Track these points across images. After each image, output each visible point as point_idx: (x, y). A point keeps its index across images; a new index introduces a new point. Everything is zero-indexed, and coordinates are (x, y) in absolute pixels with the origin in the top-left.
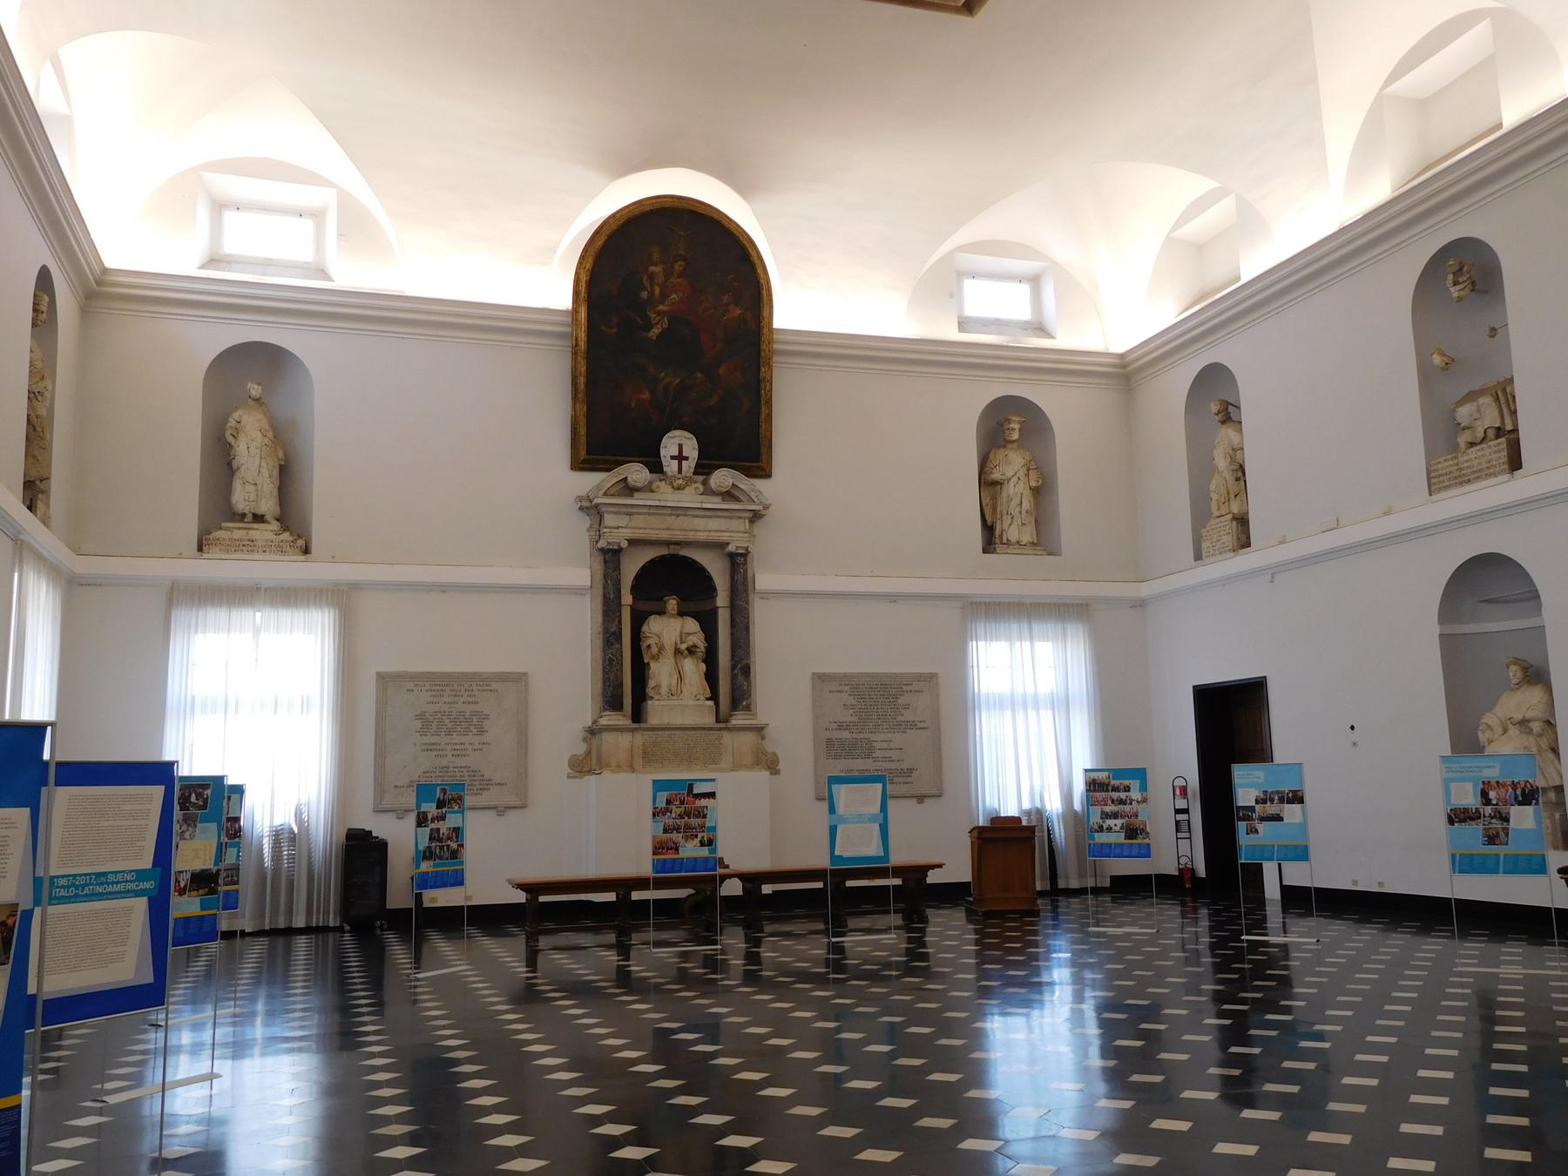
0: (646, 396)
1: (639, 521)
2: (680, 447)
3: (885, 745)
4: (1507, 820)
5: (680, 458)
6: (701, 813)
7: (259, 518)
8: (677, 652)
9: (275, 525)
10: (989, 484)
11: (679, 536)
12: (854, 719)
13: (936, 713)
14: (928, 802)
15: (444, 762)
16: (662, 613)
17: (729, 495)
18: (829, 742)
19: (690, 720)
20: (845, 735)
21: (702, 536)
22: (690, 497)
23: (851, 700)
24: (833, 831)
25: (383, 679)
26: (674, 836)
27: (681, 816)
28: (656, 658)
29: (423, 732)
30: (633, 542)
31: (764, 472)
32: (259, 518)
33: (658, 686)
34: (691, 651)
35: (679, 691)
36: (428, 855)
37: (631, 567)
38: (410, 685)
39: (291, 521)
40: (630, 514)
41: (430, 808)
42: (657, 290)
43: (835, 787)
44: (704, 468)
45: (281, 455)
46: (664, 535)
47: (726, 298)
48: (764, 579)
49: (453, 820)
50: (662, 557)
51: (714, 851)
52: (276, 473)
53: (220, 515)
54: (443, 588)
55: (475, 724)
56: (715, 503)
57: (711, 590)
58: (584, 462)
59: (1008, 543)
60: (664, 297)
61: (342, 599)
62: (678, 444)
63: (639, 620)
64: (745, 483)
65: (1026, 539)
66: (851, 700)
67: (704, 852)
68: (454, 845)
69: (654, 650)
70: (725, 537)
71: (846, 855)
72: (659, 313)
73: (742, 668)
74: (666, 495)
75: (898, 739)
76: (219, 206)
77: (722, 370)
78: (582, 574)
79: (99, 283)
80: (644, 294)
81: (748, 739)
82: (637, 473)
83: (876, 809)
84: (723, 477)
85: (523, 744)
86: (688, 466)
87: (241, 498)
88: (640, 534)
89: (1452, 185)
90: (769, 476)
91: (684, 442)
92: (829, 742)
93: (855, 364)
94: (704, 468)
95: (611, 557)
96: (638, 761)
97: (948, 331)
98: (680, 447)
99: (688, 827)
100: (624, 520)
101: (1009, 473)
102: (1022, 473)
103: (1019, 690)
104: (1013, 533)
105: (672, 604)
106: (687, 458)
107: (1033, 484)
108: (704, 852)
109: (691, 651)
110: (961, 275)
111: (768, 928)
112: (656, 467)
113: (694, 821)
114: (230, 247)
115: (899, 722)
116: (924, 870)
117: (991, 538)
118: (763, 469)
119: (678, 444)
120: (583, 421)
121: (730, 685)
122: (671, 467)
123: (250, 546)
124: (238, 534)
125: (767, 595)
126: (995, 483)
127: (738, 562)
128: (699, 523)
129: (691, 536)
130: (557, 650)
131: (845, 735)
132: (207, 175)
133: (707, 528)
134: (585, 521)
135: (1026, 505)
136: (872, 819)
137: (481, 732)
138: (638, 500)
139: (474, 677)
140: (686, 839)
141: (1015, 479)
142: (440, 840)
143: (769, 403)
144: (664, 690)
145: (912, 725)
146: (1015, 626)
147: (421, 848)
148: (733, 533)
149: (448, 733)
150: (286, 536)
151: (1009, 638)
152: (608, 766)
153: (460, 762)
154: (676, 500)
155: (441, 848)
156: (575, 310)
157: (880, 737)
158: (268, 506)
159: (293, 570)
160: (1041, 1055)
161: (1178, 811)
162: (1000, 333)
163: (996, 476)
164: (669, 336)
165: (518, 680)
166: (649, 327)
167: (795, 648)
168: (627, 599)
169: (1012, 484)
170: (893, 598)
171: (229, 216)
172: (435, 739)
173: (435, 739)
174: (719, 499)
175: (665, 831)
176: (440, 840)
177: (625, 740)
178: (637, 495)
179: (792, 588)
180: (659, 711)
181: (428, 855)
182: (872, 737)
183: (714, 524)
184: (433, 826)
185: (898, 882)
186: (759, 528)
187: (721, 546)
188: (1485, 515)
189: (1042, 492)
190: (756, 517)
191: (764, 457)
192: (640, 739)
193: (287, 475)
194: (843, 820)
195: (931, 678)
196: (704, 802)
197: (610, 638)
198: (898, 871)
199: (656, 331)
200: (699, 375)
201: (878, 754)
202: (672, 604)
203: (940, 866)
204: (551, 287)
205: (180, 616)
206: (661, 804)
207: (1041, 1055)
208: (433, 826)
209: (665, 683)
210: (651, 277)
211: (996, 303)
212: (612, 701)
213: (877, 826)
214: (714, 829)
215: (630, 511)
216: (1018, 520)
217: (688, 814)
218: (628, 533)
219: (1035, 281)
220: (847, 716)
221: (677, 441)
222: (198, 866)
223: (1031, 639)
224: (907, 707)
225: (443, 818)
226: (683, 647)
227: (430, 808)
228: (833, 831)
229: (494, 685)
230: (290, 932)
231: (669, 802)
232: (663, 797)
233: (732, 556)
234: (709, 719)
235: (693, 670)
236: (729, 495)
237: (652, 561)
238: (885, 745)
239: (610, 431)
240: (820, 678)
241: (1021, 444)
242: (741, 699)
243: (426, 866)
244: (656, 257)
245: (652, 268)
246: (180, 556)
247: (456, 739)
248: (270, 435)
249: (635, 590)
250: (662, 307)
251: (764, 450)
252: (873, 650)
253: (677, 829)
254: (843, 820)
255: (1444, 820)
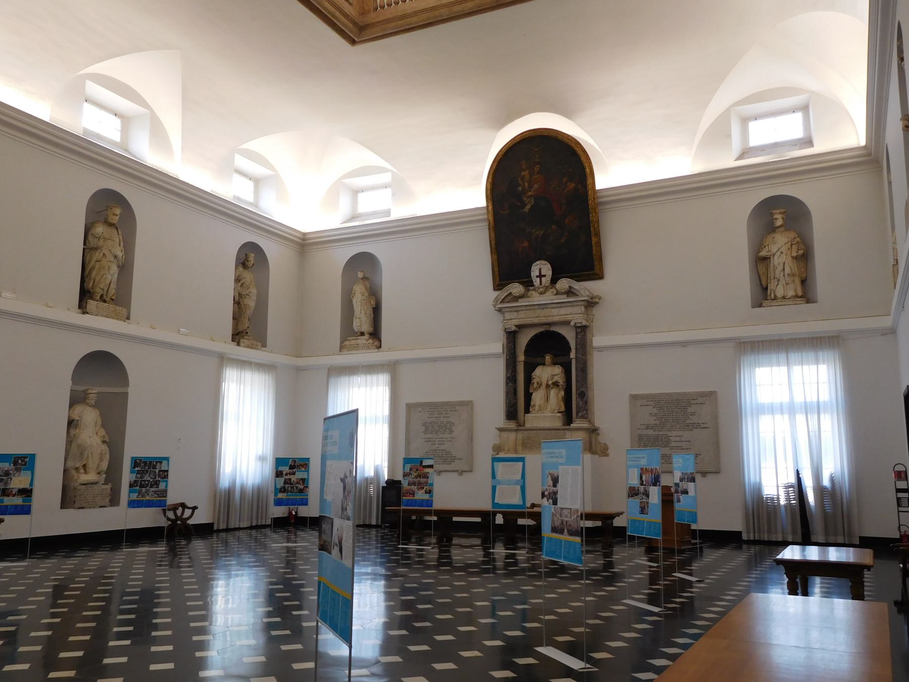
0: (526, 244)
1: (522, 314)
2: (540, 270)
3: (678, 439)
4: (648, 496)
5: (540, 276)
6: (426, 476)
7: (362, 334)
8: (548, 386)
9: (367, 336)
10: (761, 261)
11: (544, 320)
12: (658, 422)
13: (716, 417)
14: (709, 476)
15: (435, 447)
16: (544, 364)
17: (570, 292)
18: (640, 437)
19: (547, 424)
20: (651, 432)
21: (556, 319)
22: (549, 297)
23: (655, 411)
24: (494, 489)
25: (409, 407)
26: (414, 488)
27: (416, 477)
28: (535, 390)
29: (425, 432)
30: (520, 327)
31: (598, 275)
32: (362, 334)
33: (534, 406)
34: (556, 384)
35: (546, 407)
36: (283, 490)
37: (524, 340)
38: (420, 409)
39: (375, 334)
40: (517, 311)
41: (286, 469)
42: (526, 184)
43: (495, 464)
44: (554, 281)
45: (373, 302)
46: (536, 321)
47: (565, 179)
48: (598, 340)
49: (300, 475)
50: (541, 333)
51: (432, 496)
52: (370, 311)
53: (348, 333)
54: (435, 360)
55: (448, 428)
56: (563, 299)
57: (569, 349)
58: (498, 285)
59: (775, 298)
60: (530, 187)
61: (392, 369)
62: (541, 269)
63: (530, 368)
64: (577, 286)
65: (791, 293)
66: (655, 411)
67: (427, 497)
68: (301, 487)
69: (535, 385)
70: (569, 318)
71: (501, 502)
72: (528, 197)
73: (582, 395)
74: (536, 298)
75: (686, 435)
76: (356, 192)
77: (567, 221)
78: (497, 346)
79: (303, 240)
80: (520, 189)
81: (581, 435)
82: (516, 288)
83: (519, 477)
84: (564, 284)
85: (471, 438)
86: (546, 281)
87: (356, 325)
88: (522, 322)
89: (107, 158)
90: (600, 277)
91: (542, 266)
92: (640, 437)
93: (646, 201)
94: (554, 281)
95: (512, 336)
96: (520, 448)
97: (727, 160)
98: (540, 270)
99: (420, 483)
100: (514, 315)
101: (774, 250)
102: (784, 249)
103: (799, 399)
104: (780, 292)
105: (548, 358)
106: (545, 276)
107: (794, 254)
108: (427, 497)
109: (556, 384)
110: (745, 121)
111: (455, 541)
112: (528, 283)
113: (423, 480)
114: (361, 209)
115: (700, 422)
116: (611, 517)
117: (763, 294)
118: (596, 274)
119: (541, 269)
120: (496, 264)
121: (575, 404)
122: (536, 282)
123: (356, 347)
124: (353, 342)
125: (601, 349)
126: (765, 259)
127: (582, 331)
128: (555, 311)
129: (550, 320)
130: (484, 386)
131: (651, 432)
132: (347, 181)
133: (556, 315)
134: (499, 317)
135: (787, 270)
136: (517, 483)
137: (451, 432)
138: (522, 303)
139: (447, 404)
140: (419, 489)
141: (779, 253)
142: (291, 484)
143: (598, 235)
144: (537, 408)
145: (697, 426)
146: (774, 356)
147: (278, 487)
148: (576, 315)
149: (436, 433)
150: (370, 341)
151: (771, 365)
152: (504, 450)
153: (442, 447)
154: (548, 301)
155: (292, 488)
156: (488, 206)
157: (674, 433)
158: (366, 327)
159: (374, 356)
160: (234, 604)
161: (898, 491)
162: (769, 154)
163: (763, 253)
164: (544, 207)
165: (468, 405)
166: (525, 205)
167: (617, 381)
168: (521, 357)
169: (776, 257)
170: (684, 344)
171: (360, 195)
172: (430, 436)
173: (430, 436)
174: (565, 296)
175: (409, 485)
176: (291, 484)
177: (512, 436)
178: (520, 300)
179: (669, 340)
180: (532, 420)
181: (283, 490)
182: (669, 434)
183: (563, 311)
184: (288, 477)
185: (435, 518)
186: (596, 311)
187: (567, 323)
188: (102, 329)
189: (805, 257)
190: (591, 304)
191: (597, 268)
192: (520, 435)
193: (376, 311)
194: (500, 483)
195: (711, 395)
196: (427, 470)
197: (511, 379)
198: (438, 513)
199: (528, 207)
200: (554, 227)
201: (673, 444)
202: (548, 358)
203: (622, 513)
204: (476, 197)
205: (332, 381)
206: (407, 470)
207: (234, 604)
208: (288, 477)
209: (537, 404)
210: (523, 178)
211: (775, 131)
212: (511, 414)
213: (519, 487)
214: (432, 485)
215: (517, 310)
216: (782, 282)
217: (419, 476)
218: (516, 322)
219: (805, 109)
220: (652, 421)
221: (538, 267)
222: (22, 487)
223: (788, 364)
224: (693, 414)
225: (294, 474)
226: (550, 383)
227: (286, 469)
228: (494, 489)
229: (457, 408)
230: (370, 526)
231: (411, 470)
232: (408, 466)
233: (576, 327)
234: (558, 424)
235: (556, 397)
236: (570, 292)
237: (536, 336)
238: (678, 439)
239: (509, 269)
240: (634, 398)
241: (786, 227)
242: (585, 411)
243: (280, 495)
244: (524, 167)
245: (523, 173)
246: (334, 354)
247: (441, 436)
248: (367, 294)
249: (527, 352)
250: (530, 193)
251: (596, 263)
252: (671, 377)
253: (414, 484)
254: (500, 483)
255: (625, 494)
